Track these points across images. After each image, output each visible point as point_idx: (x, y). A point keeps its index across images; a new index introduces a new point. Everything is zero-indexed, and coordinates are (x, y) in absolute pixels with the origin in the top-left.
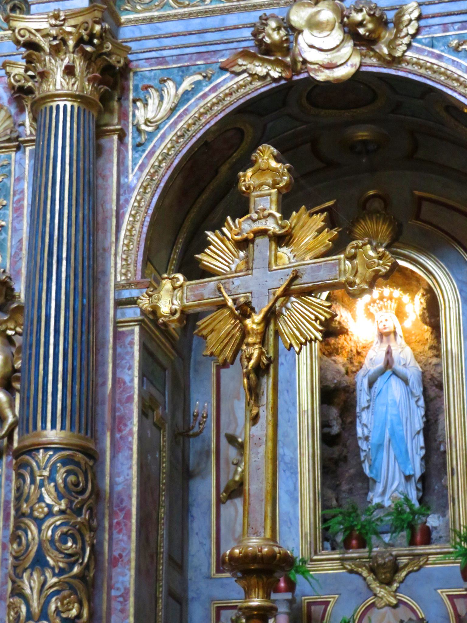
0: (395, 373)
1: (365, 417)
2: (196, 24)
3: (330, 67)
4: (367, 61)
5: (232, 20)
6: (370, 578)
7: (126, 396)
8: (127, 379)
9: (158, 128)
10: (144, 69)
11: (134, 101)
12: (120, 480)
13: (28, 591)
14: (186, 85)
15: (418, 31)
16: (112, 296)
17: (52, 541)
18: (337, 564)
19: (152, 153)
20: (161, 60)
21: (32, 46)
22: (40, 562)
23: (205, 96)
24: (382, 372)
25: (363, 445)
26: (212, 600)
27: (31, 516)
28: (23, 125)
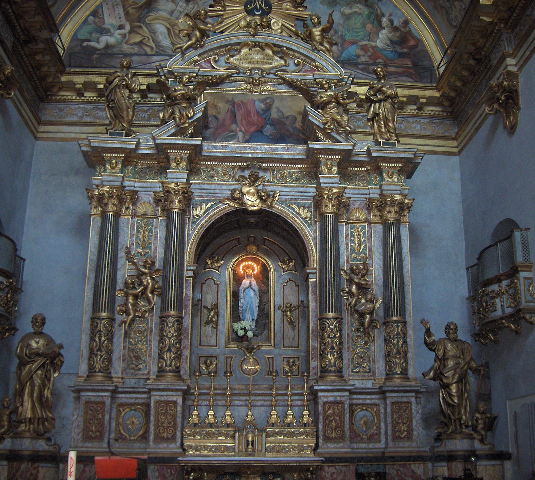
0: (252, 288)
1: (242, 301)
2: (213, 187)
3: (253, 206)
4: (264, 206)
5: (224, 187)
6: (246, 351)
7: (188, 299)
8: (188, 294)
9: (200, 217)
10: (196, 198)
11: (193, 208)
12: (185, 324)
13: (166, 358)
14: (209, 205)
15: (278, 199)
16: (185, 268)
17: (173, 344)
18: (236, 346)
19: (198, 225)
20: (202, 197)
21: (168, 192)
22: (169, 350)
23: (214, 210)
24: (248, 288)
25: (241, 309)
26: (198, 354)
27: (167, 336)
28: (158, 210)
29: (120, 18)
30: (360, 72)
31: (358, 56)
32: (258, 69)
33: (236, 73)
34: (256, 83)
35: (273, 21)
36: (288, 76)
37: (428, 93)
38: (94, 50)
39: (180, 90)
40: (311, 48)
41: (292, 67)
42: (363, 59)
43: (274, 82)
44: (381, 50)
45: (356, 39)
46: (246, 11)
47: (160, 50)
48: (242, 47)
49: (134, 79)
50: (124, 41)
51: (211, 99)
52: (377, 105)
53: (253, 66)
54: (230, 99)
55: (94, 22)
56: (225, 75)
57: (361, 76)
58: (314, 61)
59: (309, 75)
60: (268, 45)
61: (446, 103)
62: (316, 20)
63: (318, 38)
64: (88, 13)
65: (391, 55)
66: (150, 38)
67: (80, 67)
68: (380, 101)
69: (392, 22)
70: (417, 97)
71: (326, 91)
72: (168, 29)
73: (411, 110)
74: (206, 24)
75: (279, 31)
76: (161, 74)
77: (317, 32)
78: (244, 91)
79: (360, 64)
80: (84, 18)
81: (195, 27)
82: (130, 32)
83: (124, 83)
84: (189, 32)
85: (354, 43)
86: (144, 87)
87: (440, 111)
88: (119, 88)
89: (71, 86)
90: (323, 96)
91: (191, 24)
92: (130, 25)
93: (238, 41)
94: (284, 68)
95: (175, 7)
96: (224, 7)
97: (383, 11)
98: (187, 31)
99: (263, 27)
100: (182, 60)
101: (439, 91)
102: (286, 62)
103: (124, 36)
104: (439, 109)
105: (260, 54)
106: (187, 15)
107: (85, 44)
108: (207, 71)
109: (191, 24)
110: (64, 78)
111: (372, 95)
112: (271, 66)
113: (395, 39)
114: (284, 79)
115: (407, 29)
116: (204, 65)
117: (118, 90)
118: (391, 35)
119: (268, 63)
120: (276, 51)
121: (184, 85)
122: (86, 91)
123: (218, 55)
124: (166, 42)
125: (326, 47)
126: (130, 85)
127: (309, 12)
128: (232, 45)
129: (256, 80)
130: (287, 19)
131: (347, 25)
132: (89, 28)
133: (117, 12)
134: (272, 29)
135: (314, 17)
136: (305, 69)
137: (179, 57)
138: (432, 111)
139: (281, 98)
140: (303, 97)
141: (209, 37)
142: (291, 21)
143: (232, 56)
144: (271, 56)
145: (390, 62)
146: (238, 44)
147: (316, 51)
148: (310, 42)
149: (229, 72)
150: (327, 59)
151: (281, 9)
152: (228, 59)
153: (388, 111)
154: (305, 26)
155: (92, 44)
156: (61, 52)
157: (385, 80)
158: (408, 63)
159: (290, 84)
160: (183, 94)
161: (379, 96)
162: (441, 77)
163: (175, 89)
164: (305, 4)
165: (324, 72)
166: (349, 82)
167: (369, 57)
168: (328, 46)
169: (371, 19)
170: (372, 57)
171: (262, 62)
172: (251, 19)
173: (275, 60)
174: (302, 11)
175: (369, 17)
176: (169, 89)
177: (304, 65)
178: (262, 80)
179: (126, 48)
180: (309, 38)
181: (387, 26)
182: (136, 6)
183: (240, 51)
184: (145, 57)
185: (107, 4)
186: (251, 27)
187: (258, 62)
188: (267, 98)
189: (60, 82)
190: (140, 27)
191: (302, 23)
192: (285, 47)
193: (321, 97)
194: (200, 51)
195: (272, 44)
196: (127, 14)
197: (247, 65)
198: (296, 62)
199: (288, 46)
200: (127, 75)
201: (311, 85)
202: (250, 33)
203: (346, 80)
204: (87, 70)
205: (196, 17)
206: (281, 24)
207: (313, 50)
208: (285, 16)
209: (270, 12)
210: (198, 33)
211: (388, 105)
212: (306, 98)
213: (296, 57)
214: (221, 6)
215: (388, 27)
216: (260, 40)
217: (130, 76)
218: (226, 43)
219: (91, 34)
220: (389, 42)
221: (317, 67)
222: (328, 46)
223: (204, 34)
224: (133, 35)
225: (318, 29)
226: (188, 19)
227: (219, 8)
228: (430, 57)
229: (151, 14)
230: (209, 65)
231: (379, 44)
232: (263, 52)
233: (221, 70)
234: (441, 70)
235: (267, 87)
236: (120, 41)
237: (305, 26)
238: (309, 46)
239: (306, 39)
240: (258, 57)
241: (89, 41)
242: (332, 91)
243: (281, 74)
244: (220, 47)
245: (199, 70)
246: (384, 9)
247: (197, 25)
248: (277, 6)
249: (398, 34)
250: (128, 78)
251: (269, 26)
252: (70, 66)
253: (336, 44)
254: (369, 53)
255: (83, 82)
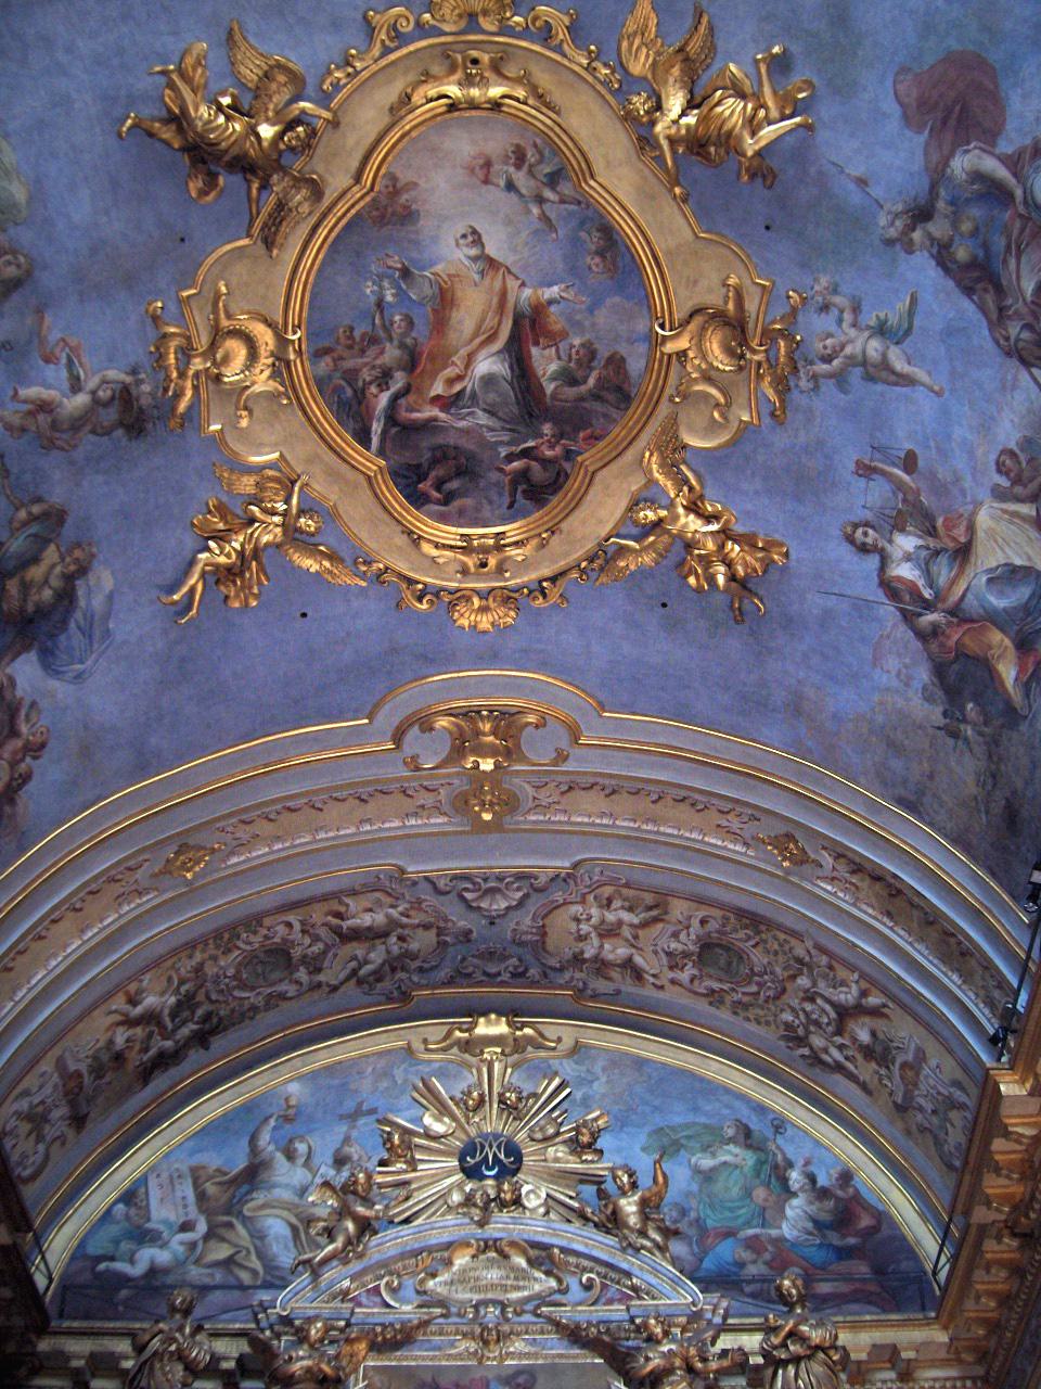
29: (185, 1206)
30: (750, 1300)
31: (742, 1265)
32: (495, 1302)
33: (442, 1316)
34: (487, 1337)
35: (524, 1190)
36: (565, 1314)
37: (918, 1335)
38: (124, 1280)
39: (302, 1358)
40: (618, 1246)
41: (576, 1292)
42: (752, 1270)
43: (534, 1333)
44: (793, 1245)
45: (730, 1225)
46: (463, 1170)
47: (273, 1276)
48: (453, 1253)
49: (198, 1338)
50: (193, 1258)
51: (382, 1382)
52: (791, 1370)
53: (482, 1296)
54: (429, 1379)
55: (127, 1217)
56: (416, 1322)
57: (751, 1309)
58: (628, 1275)
59: (618, 1310)
60: (513, 1244)
61: (968, 1357)
62: (625, 1179)
63: (633, 1220)
64: (114, 1196)
65: (819, 1256)
66: (252, 1249)
67: (87, 1317)
68: (796, 1360)
69: (812, 1179)
70: (894, 1350)
71: (659, 1342)
72: (294, 1229)
73: (884, 1382)
74: (367, 1201)
75: (542, 1210)
76: (264, 1324)
77: (629, 1206)
78: (462, 1360)
79: (749, 1282)
80: (103, 1207)
81: (344, 1212)
82: (207, 1237)
83: (173, 1348)
84: (331, 1226)
85: (729, 1233)
86: (229, 1365)
87: (955, 1379)
88: (162, 1360)
89: (57, 1364)
90: (651, 1355)
91: (336, 1205)
92: (209, 1222)
93: (446, 1238)
94: (557, 1297)
95: (310, 1177)
96: (413, 1164)
97: (789, 1156)
98: (325, 1220)
99: (503, 1205)
100: (313, 1289)
101: (945, 1328)
102: (560, 1281)
103: (192, 1245)
104: (953, 1373)
105: (499, 1267)
106: (326, 1184)
107: (102, 1266)
108: (373, 1314)
109: (336, 1205)
110: (44, 1345)
111: (775, 1348)
112: (526, 1293)
113: (825, 1217)
114: (557, 1324)
115: (851, 1190)
116: (364, 1300)
117: (158, 1366)
118: (814, 1208)
119: (518, 1288)
120: (537, 1258)
121: (312, 1346)
122: (94, 1376)
123: (399, 1276)
124: (286, 1257)
125: (653, 1241)
126: (187, 1352)
127: (609, 1161)
128: (430, 1250)
129: (489, 1330)
130: (560, 1181)
131: (709, 1197)
132: (113, 1230)
133: (179, 1194)
134: (525, 1208)
135: (620, 1173)
136: (609, 1295)
137: (306, 1282)
138: (935, 1380)
139: (553, 1369)
140: (607, 1367)
141: (376, 1233)
142: (568, 1186)
143: (434, 1276)
144: (523, 1270)
145: (818, 1271)
146: (449, 1246)
147: (630, 1251)
148: (614, 1231)
149: (424, 1313)
150: (659, 1268)
151: (545, 1160)
152: (422, 1281)
153: (818, 1382)
154: (602, 1194)
155: (120, 1266)
156: (40, 1281)
157: (803, 1307)
158: (862, 1269)
159: (574, 1335)
160: (308, 1370)
161: (792, 1348)
162: (945, 1290)
163: (291, 1358)
164: (598, 1145)
165: (654, 1298)
166: (718, 1320)
167: (766, 1263)
168: (658, 1238)
169: (763, 1176)
170: (774, 1264)
171: (502, 1286)
172: (475, 1187)
173: (535, 1279)
174: (592, 1162)
175: (758, 1176)
176: (275, 1356)
177: (604, 1286)
178: (506, 1328)
179: (195, 1273)
180: (612, 1222)
181: (801, 1189)
182: (226, 1178)
183: (449, 1263)
184: (236, 1294)
185: (158, 1176)
186: (475, 1205)
187: (493, 1287)
188: (520, 1371)
189: (34, 1354)
190: (230, 1225)
191: (595, 1187)
192: (557, 1246)
193: (648, 1359)
194: (355, 1266)
195: (526, 1241)
196: (201, 1197)
197: (468, 1296)
198: (584, 1280)
199: (564, 1243)
200: (181, 1329)
201: (623, 1335)
202: (472, 1219)
203: (708, 1315)
204: (98, 1324)
205: (348, 1190)
206: (544, 1195)
207: (623, 1250)
208: (553, 1176)
209: (518, 1170)
210: (350, 1226)
211: (817, 1368)
212: (612, 1367)
213: (584, 1270)
214: (405, 1162)
215: (805, 1191)
216: (497, 1235)
217: (187, 1330)
218: (416, 1246)
219: (117, 1242)
220: (810, 1225)
221: (635, 1288)
222: (658, 1238)
223: (366, 1227)
224: (212, 1244)
225: (631, 1200)
226: (328, 1193)
227: (401, 1166)
228: (913, 1252)
229: (254, 1195)
230: (378, 1299)
231: (787, 1230)
232: (505, 1262)
233: (407, 1310)
234: (943, 1275)
235: (518, 1346)
236: (182, 1257)
237: (602, 1194)
238: (611, 1240)
239: (604, 1226)
240: (493, 1275)
241: (112, 1259)
242: (674, 1340)
243: (551, 1312)
244: (403, 1256)
245: (352, 1313)
246: (790, 1151)
247: (349, 1208)
248: (533, 1153)
249: (831, 1203)
250: (183, 1335)
251: (517, 1202)
252: (61, 1316)
253: (676, 1233)
254: (767, 1256)
255: (87, 1354)
